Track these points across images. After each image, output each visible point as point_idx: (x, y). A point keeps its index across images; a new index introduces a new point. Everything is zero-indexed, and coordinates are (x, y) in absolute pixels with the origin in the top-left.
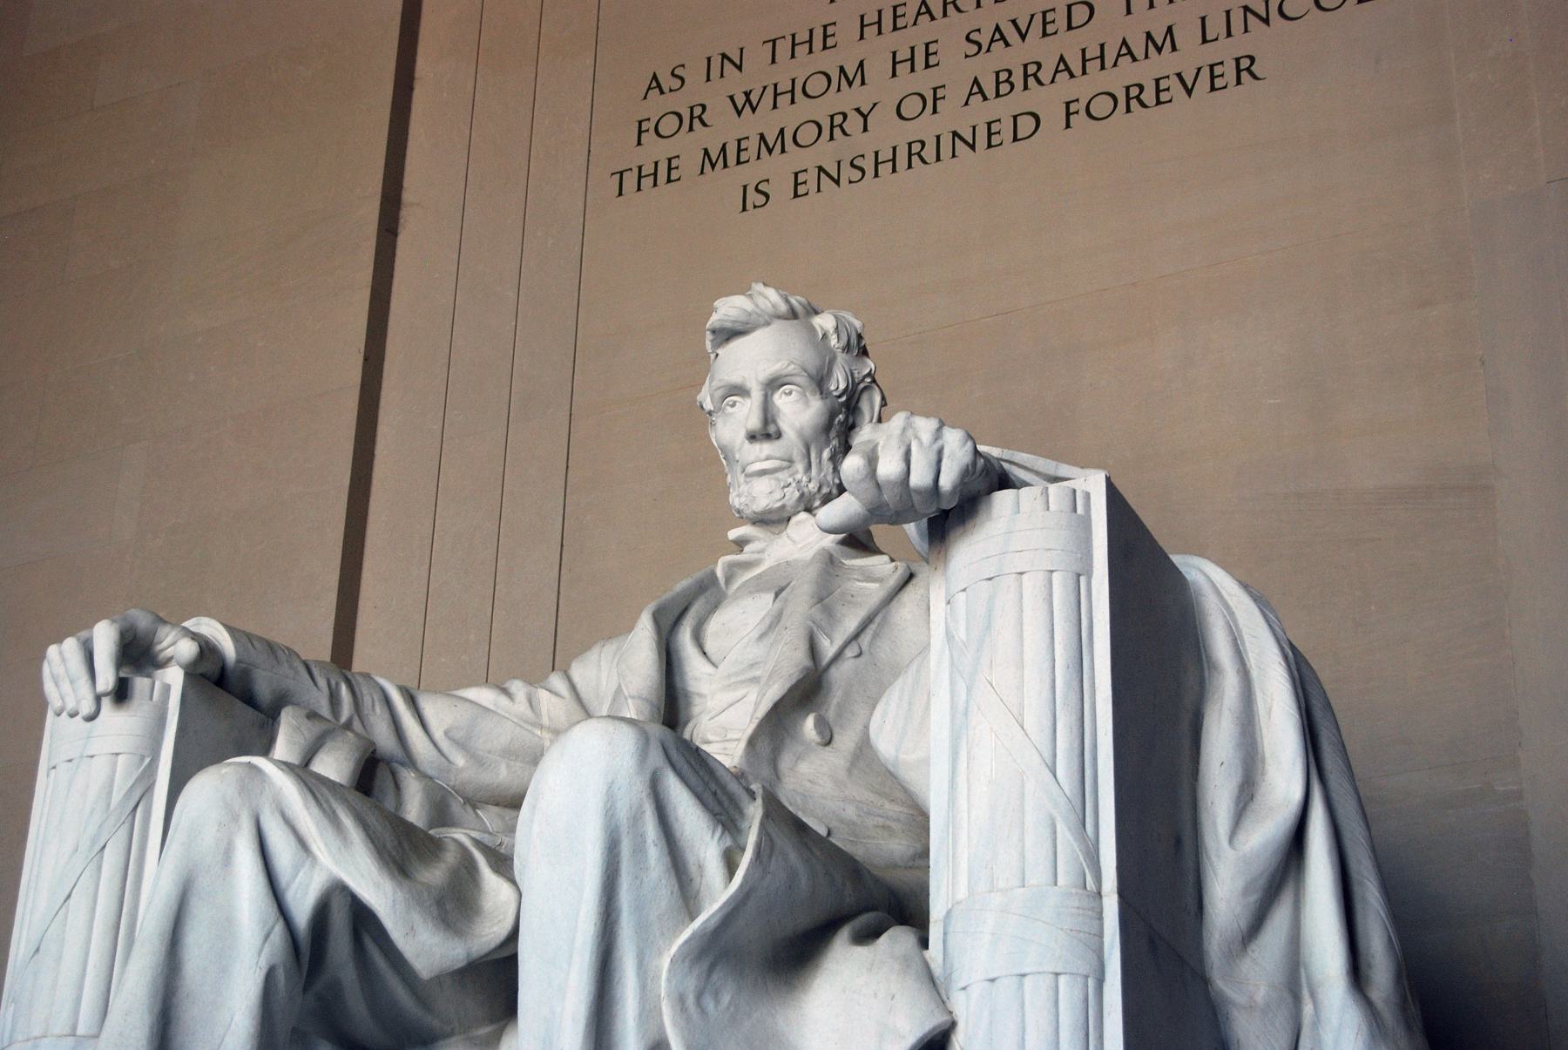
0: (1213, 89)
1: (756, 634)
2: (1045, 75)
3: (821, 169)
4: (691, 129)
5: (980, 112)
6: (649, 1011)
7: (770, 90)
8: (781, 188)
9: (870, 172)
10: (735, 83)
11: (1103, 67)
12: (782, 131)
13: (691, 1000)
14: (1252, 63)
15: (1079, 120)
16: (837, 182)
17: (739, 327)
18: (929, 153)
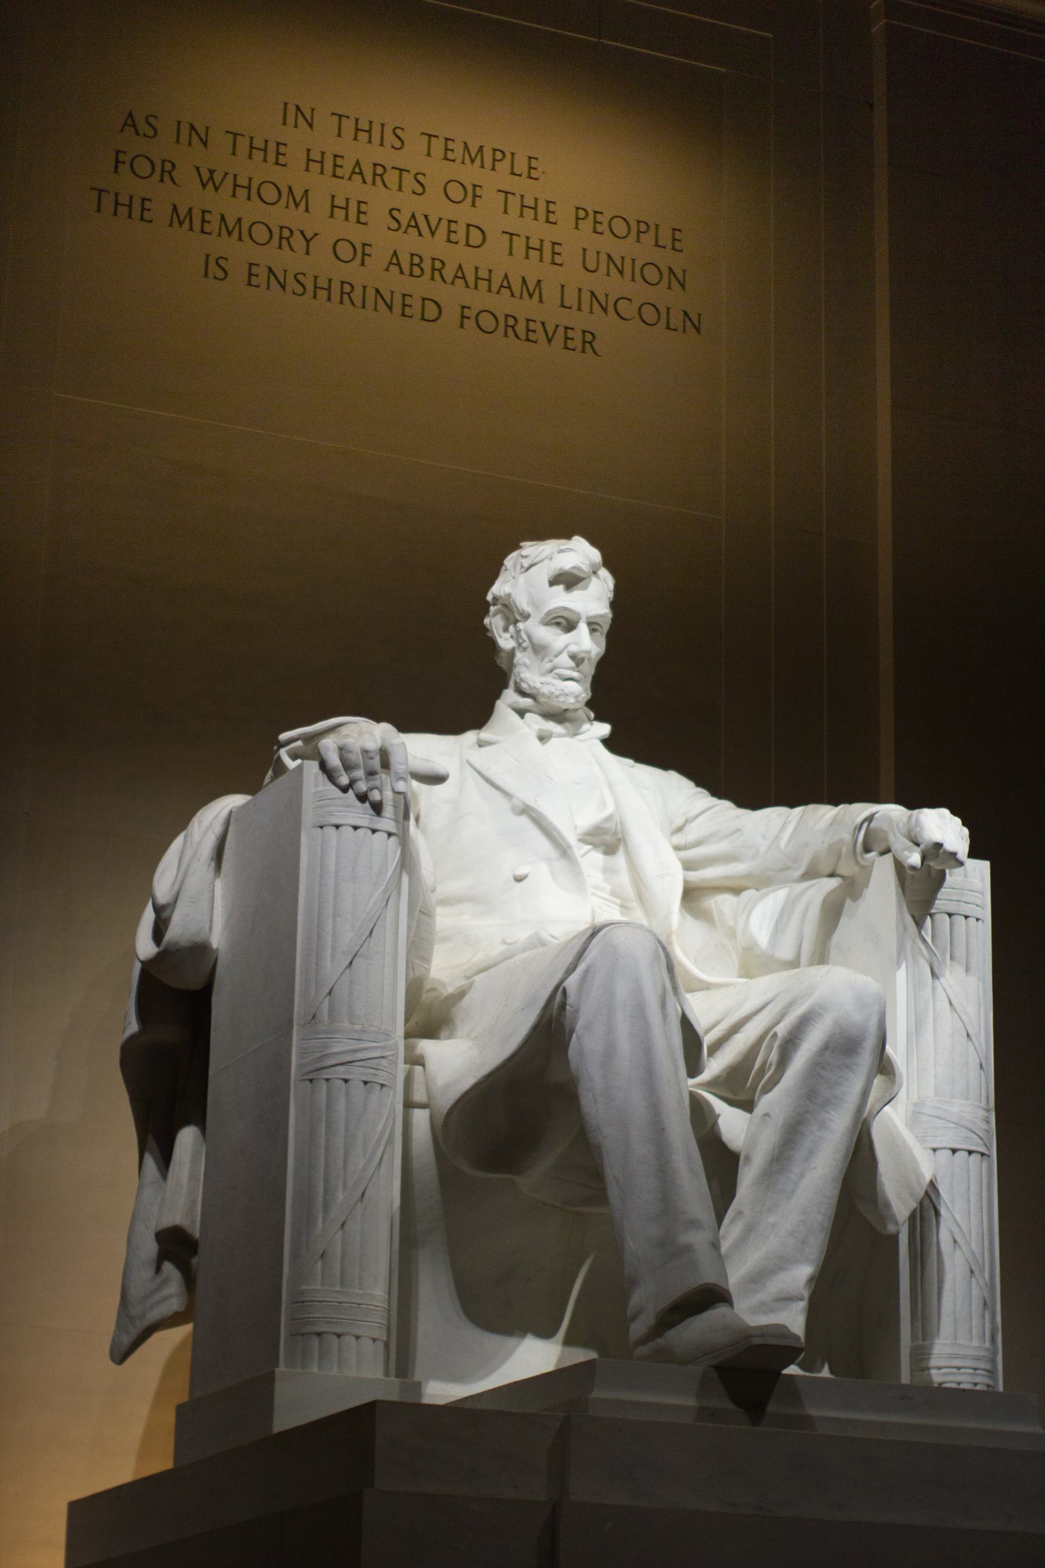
2: (449, 273)
3: (270, 270)
4: (162, 180)
7: (230, 177)
11: (490, 290)
12: (240, 220)
15: (470, 324)
16: (283, 287)
18: (357, 296)
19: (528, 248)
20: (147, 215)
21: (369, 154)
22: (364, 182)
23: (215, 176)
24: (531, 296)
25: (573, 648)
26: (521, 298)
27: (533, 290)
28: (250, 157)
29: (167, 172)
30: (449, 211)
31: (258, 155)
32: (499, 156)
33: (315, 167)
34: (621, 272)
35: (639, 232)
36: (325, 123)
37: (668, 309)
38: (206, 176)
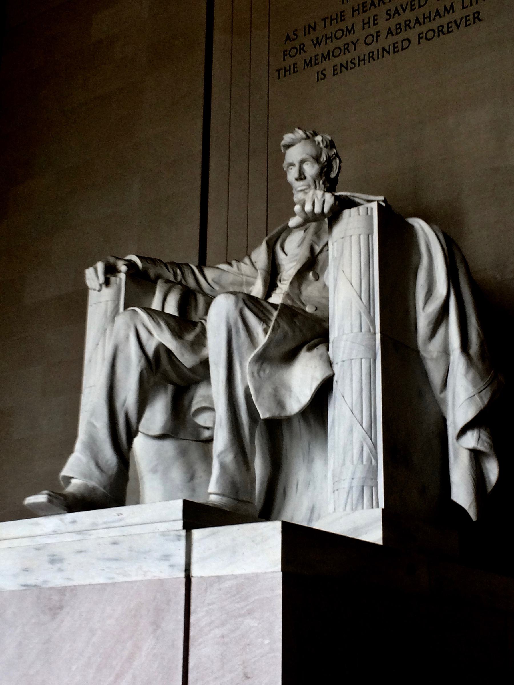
1: (297, 246)
2: (412, 25)
5: (392, 39)
6: (243, 378)
8: (329, 72)
9: (357, 65)
10: (313, 35)
13: (256, 374)
14: (479, 15)
15: (423, 40)
17: (290, 144)
18: (375, 56)
29: (302, 48)
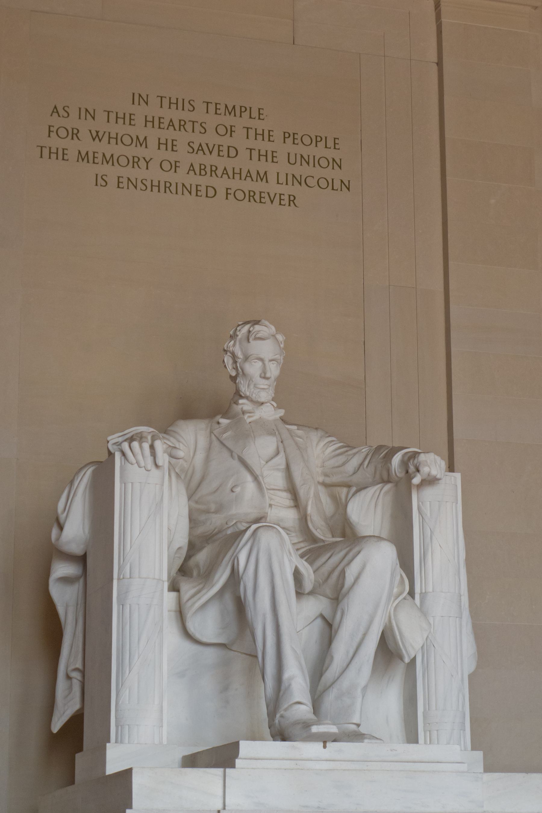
0: (280, 204)
3: (129, 179)
4: (72, 139)
5: (192, 180)
7: (107, 134)
8: (112, 181)
11: (241, 179)
12: (112, 155)
15: (231, 197)
16: (136, 187)
18: (173, 188)
19: (259, 155)
20: (66, 157)
21: (176, 115)
22: (175, 130)
23: (99, 134)
24: (262, 180)
25: (263, 375)
26: (257, 181)
27: (263, 177)
28: (117, 122)
29: (75, 134)
30: (219, 140)
31: (120, 121)
32: (243, 109)
33: (149, 124)
34: (308, 163)
35: (317, 142)
36: (154, 101)
37: (333, 180)
38: (94, 134)
